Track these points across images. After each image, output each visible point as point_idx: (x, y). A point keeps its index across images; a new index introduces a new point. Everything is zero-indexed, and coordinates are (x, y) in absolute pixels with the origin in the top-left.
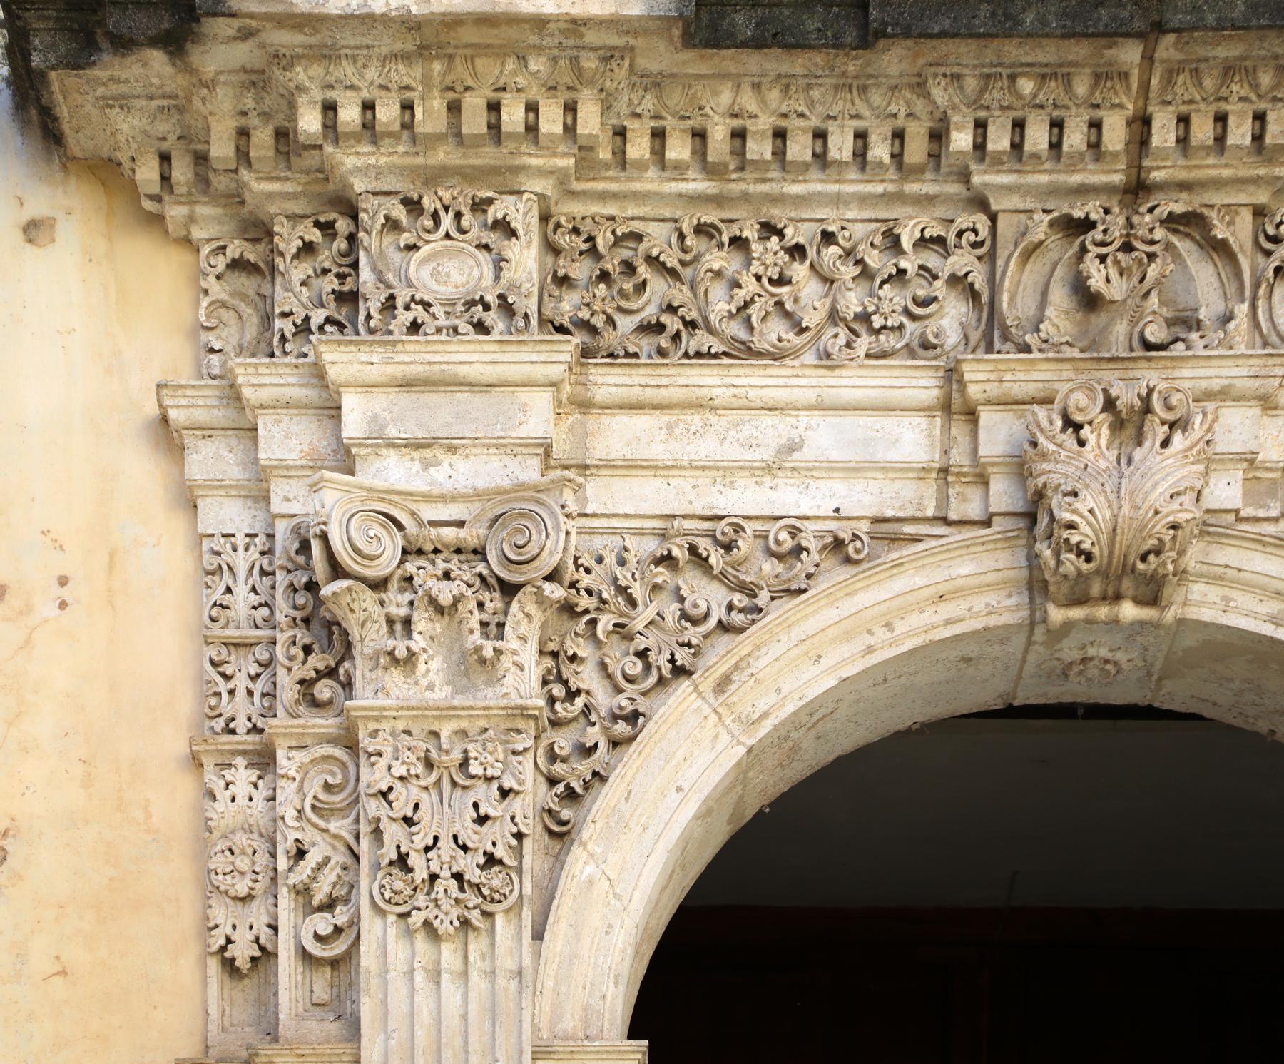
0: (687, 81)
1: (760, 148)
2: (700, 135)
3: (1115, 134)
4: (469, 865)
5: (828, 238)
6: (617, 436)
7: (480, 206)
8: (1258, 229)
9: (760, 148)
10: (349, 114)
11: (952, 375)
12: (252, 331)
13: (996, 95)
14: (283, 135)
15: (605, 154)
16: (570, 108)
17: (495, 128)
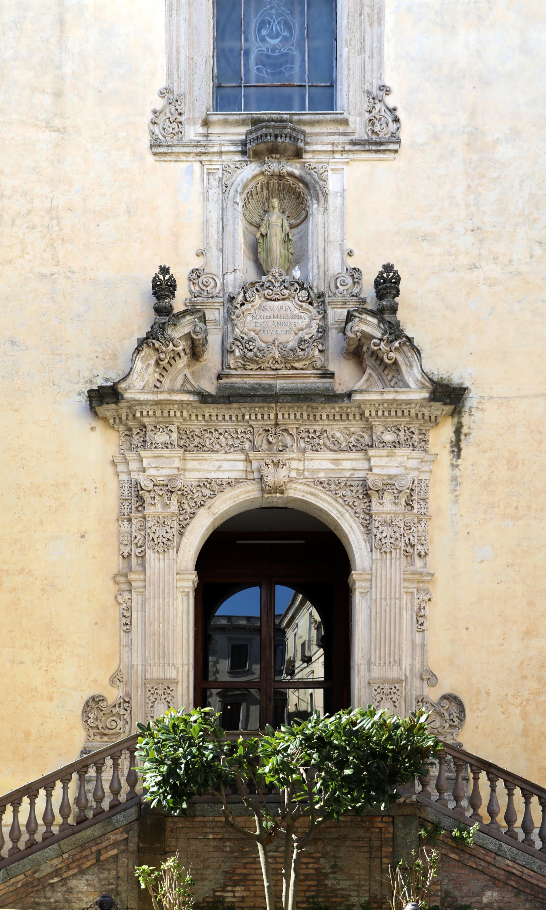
0: (201, 408)
1: (214, 418)
2: (204, 415)
3: (272, 416)
5: (226, 432)
6: (190, 465)
7: (167, 427)
8: (297, 431)
9: (214, 418)
10: (145, 413)
11: (247, 455)
12: (129, 446)
13: (252, 410)
14: (134, 416)
15: (188, 419)
16: (182, 412)
17: (169, 415)
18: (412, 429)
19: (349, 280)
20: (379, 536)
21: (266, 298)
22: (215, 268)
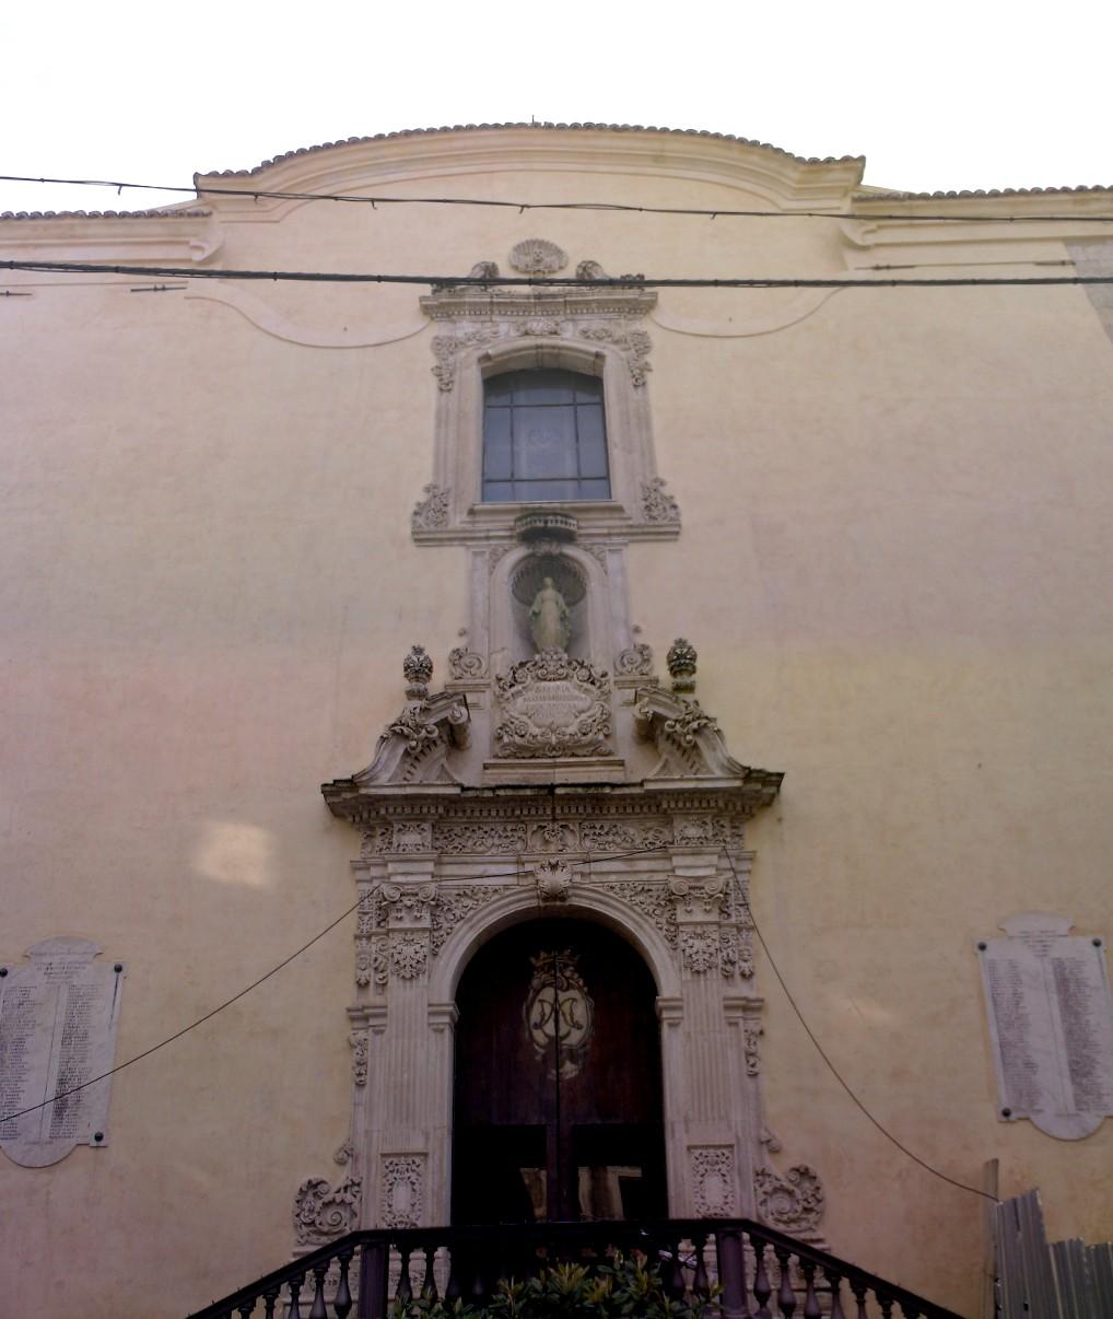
3: (549, 812)
4: (414, 963)
5: (492, 829)
7: (418, 826)
18: (722, 822)
19: (638, 658)
20: (688, 951)
21: (539, 678)
22: (481, 648)
